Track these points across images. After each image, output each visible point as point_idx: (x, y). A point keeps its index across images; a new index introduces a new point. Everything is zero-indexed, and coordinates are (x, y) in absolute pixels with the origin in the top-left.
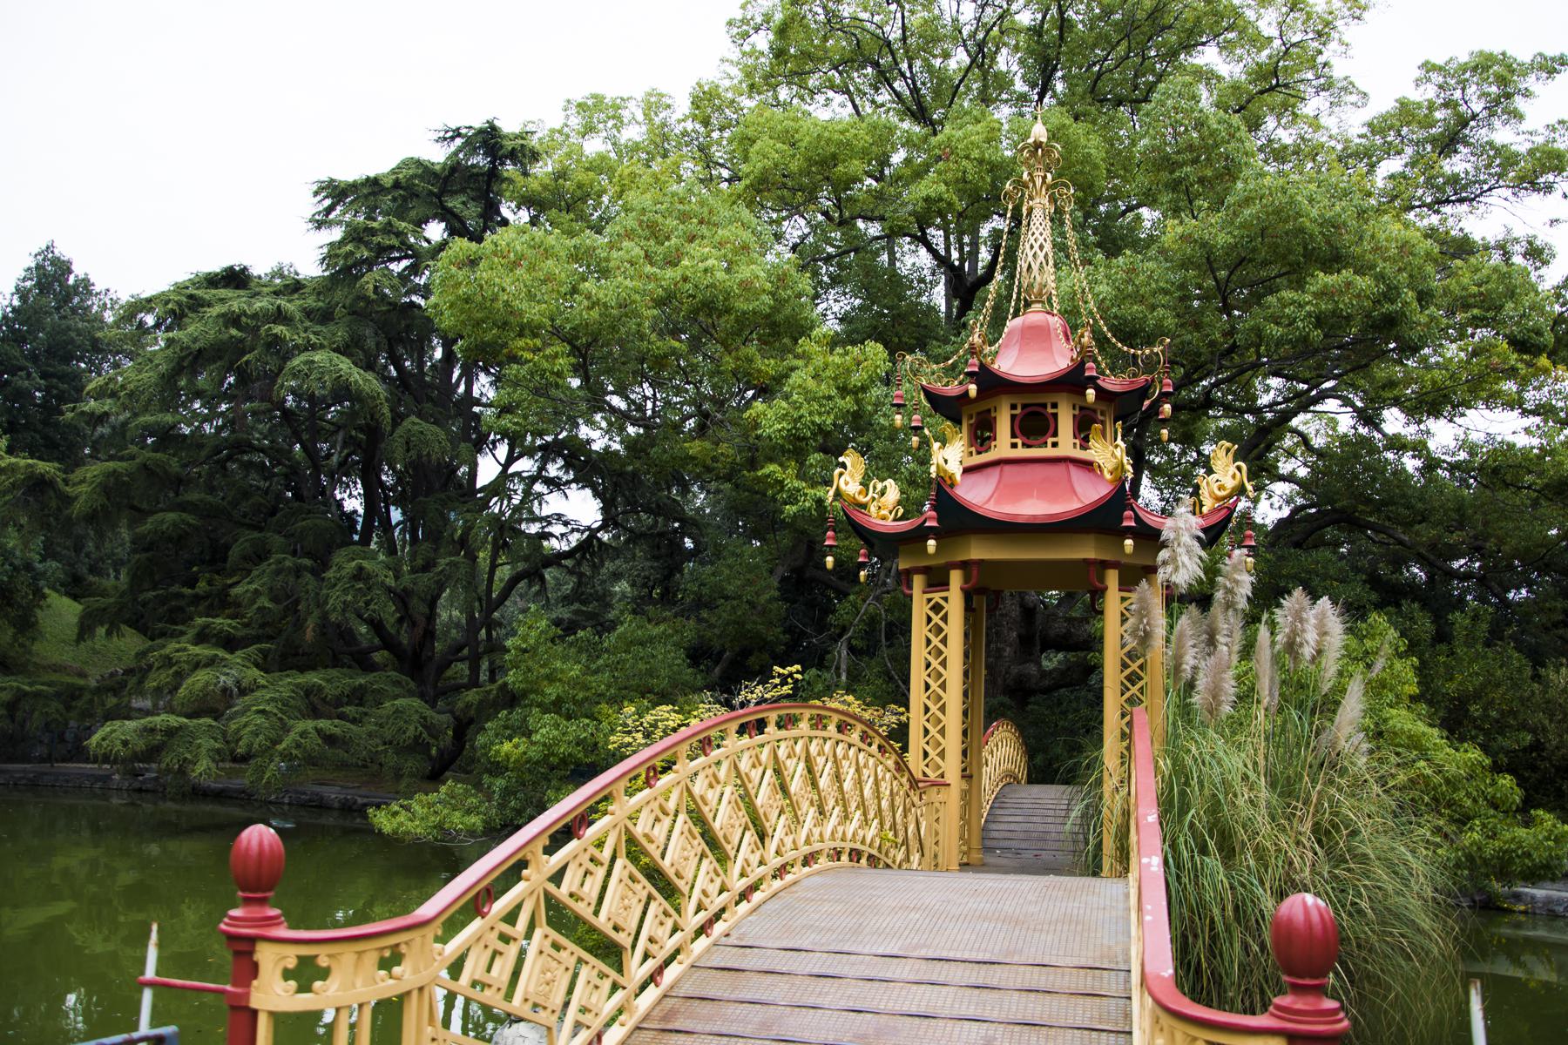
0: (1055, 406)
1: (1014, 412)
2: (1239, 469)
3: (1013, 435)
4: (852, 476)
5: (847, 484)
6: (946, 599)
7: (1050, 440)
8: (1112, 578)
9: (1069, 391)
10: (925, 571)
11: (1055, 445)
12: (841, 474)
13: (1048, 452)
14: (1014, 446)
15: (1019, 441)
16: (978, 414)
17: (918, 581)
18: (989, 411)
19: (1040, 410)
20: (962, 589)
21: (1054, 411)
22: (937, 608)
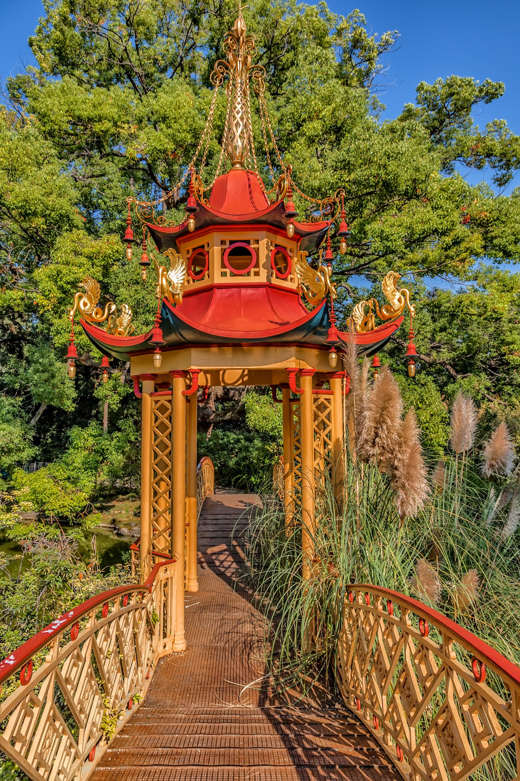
0: (257, 242)
1: (224, 247)
2: (404, 294)
3: (223, 266)
4: (90, 299)
5: (85, 305)
6: (170, 401)
7: (253, 270)
8: (307, 382)
9: (269, 230)
10: (153, 377)
11: (257, 274)
12: (80, 297)
13: (252, 279)
14: (223, 274)
15: (228, 271)
16: (194, 249)
17: (148, 385)
18: (203, 247)
19: (236, 272)
20: (183, 393)
21: (256, 246)
22: (163, 409)
